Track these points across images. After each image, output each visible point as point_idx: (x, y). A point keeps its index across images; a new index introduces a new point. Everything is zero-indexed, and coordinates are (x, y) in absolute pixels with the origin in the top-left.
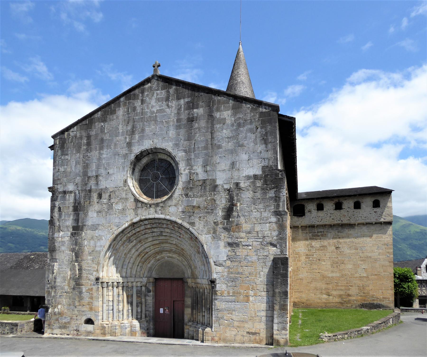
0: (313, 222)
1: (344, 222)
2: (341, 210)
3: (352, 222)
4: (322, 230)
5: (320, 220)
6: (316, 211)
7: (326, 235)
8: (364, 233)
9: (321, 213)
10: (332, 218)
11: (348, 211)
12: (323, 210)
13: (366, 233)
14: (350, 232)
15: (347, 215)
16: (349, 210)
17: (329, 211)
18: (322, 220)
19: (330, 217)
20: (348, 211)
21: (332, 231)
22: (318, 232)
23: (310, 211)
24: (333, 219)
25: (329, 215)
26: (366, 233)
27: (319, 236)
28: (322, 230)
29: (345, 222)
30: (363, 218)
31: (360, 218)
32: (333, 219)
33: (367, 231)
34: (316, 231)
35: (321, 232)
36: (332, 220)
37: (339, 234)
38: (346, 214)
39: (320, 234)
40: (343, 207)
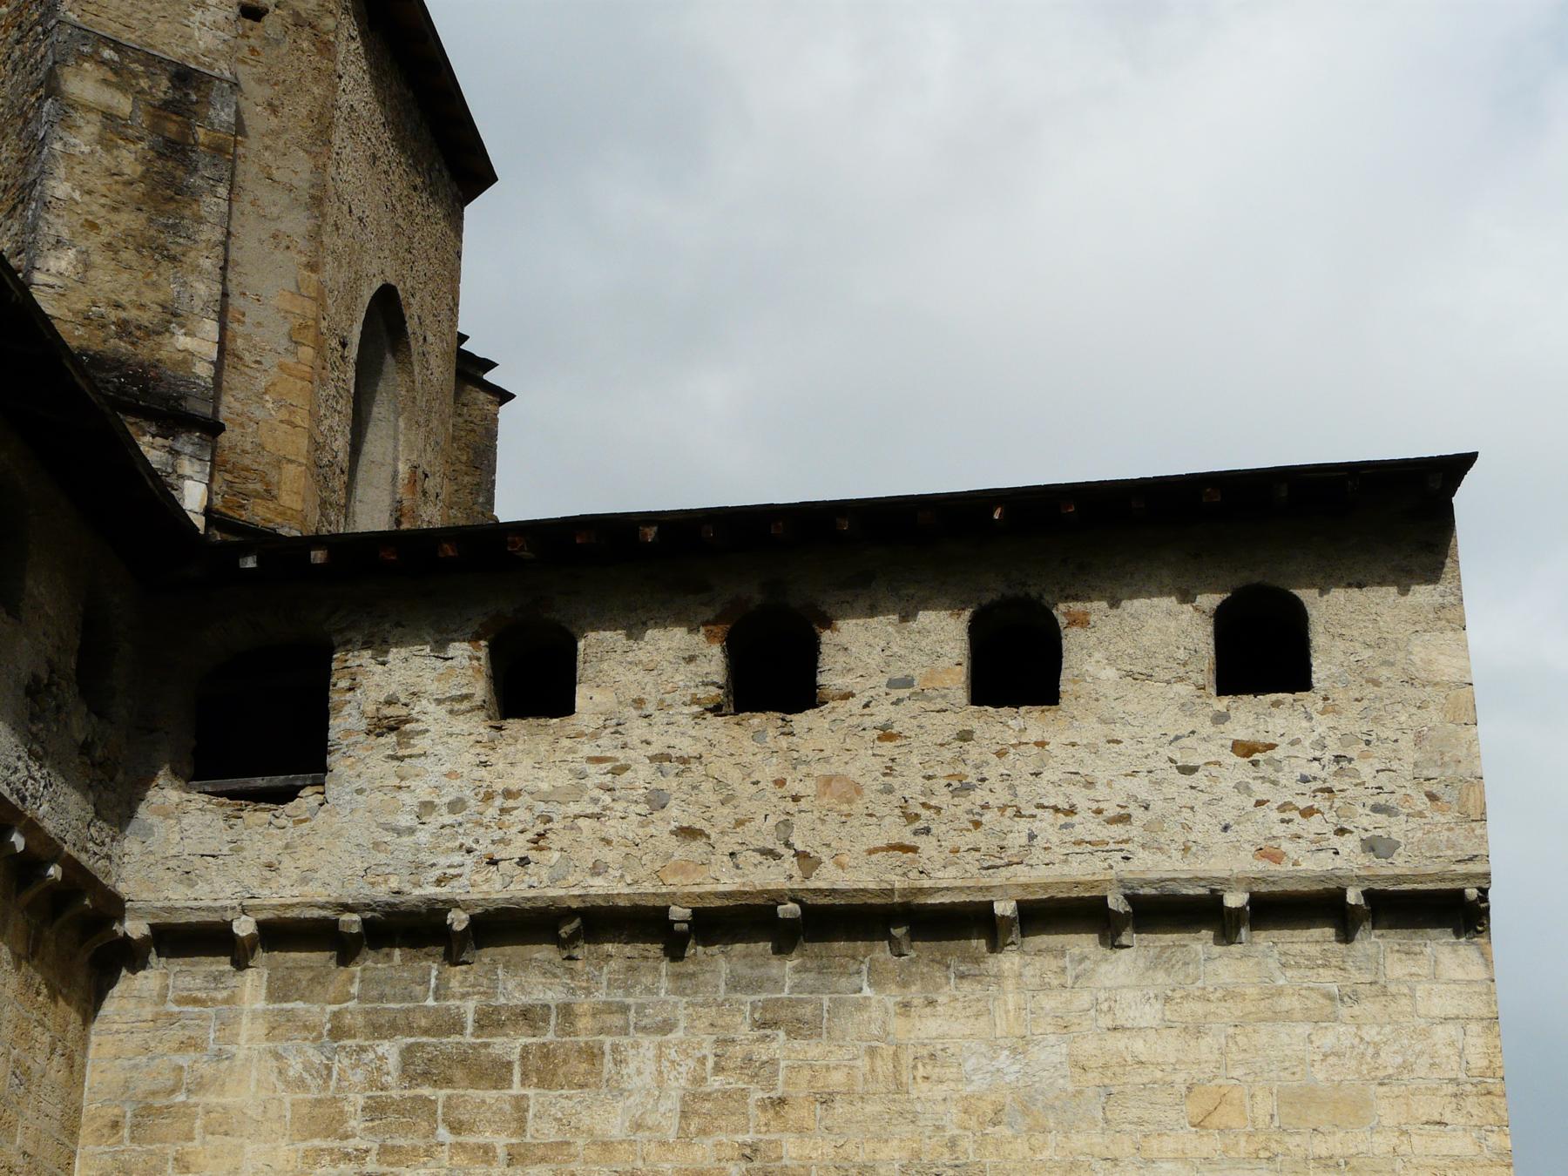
0: (417, 867)
1: (829, 877)
2: (801, 720)
3: (945, 876)
4: (548, 992)
5: (519, 847)
6: (478, 726)
7: (592, 1055)
8: (1119, 1042)
9: (533, 756)
10: (677, 814)
11: (886, 734)
12: (564, 707)
13: (1139, 1046)
14: (929, 1026)
15: (872, 783)
16: (902, 720)
17: (637, 729)
18: (538, 841)
19: (657, 801)
20: (886, 734)
21: (680, 1009)
22: (489, 1021)
23: (390, 725)
24: (688, 833)
25: (642, 774)
26: (1139, 1046)
27: (497, 1074)
28: (548, 992)
29: (854, 871)
30: (1087, 826)
31: (1046, 824)
32: (688, 833)
33: (1150, 1014)
34: (469, 1008)
35: (529, 1017)
36: (682, 851)
37: (779, 1046)
38: (864, 764)
39: (510, 1045)
40: (830, 677)
